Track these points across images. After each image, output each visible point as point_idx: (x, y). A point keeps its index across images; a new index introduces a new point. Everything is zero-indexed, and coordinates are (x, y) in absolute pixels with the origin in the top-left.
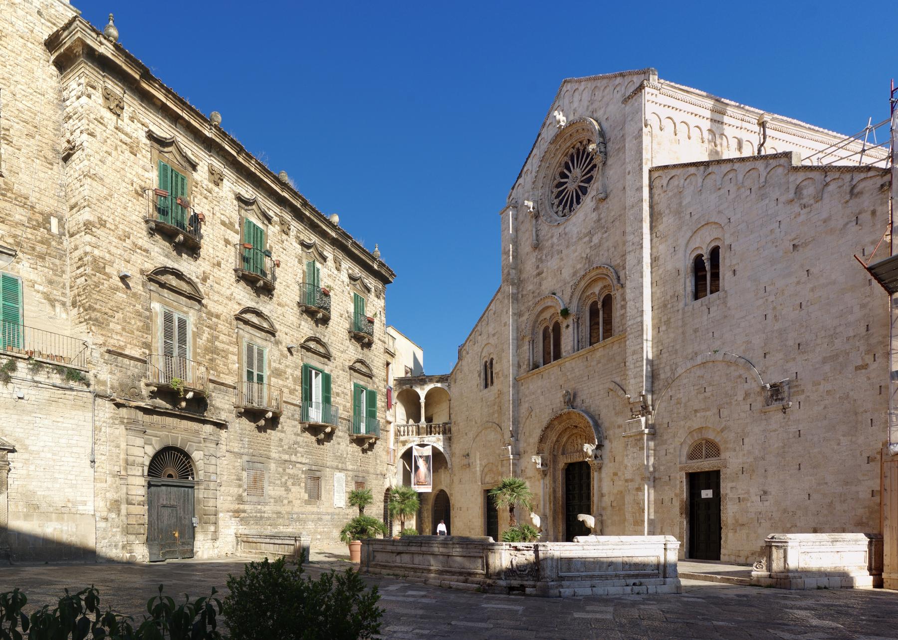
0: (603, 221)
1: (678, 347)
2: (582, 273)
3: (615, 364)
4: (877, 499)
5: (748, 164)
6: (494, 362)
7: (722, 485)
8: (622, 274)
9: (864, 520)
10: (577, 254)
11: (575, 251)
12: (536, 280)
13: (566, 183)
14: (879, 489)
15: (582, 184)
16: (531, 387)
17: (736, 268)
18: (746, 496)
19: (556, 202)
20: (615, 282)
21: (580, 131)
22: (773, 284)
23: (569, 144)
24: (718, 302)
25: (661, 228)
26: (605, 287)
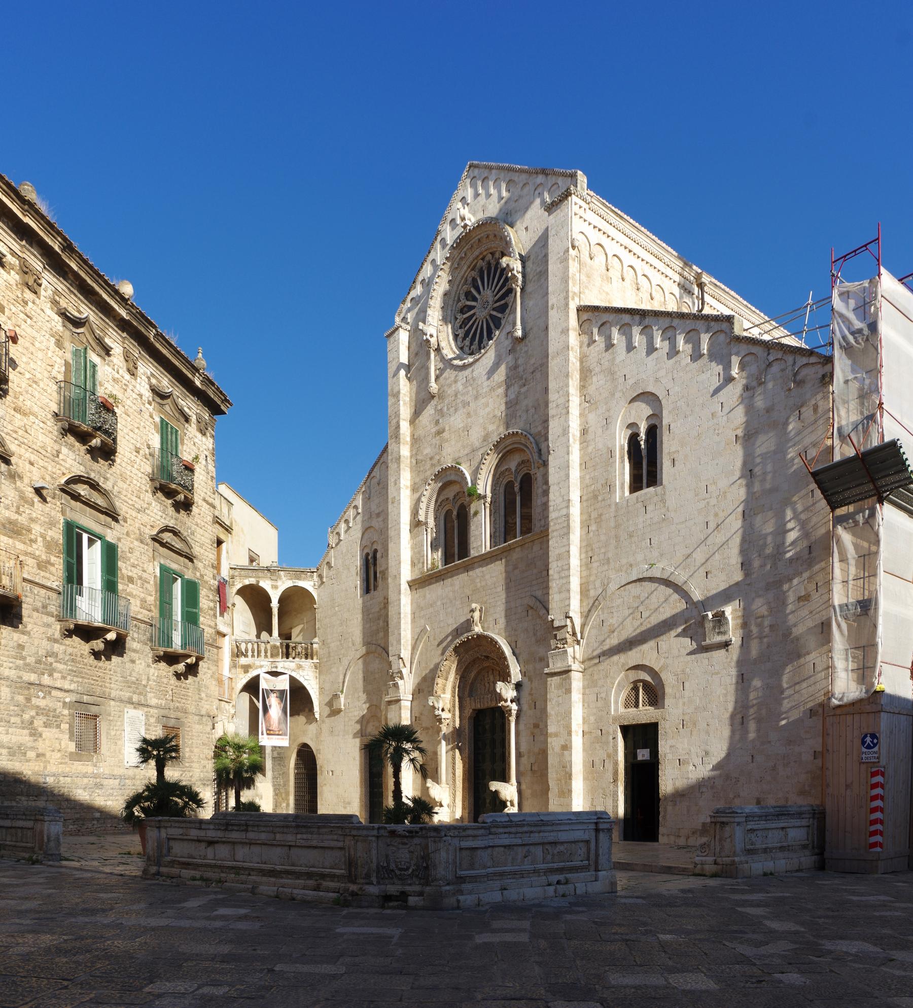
0: (521, 369)
1: (610, 555)
3: (535, 571)
4: (819, 762)
5: (688, 322)
6: (379, 555)
7: (661, 743)
8: (543, 446)
9: (807, 788)
10: (487, 410)
11: (487, 405)
12: (436, 441)
13: (473, 307)
14: (820, 749)
15: (494, 313)
16: (428, 596)
17: (675, 456)
18: (687, 757)
19: (461, 332)
20: (536, 456)
21: (491, 237)
22: (715, 483)
23: (477, 253)
24: (655, 499)
25: (591, 389)
26: (523, 462)
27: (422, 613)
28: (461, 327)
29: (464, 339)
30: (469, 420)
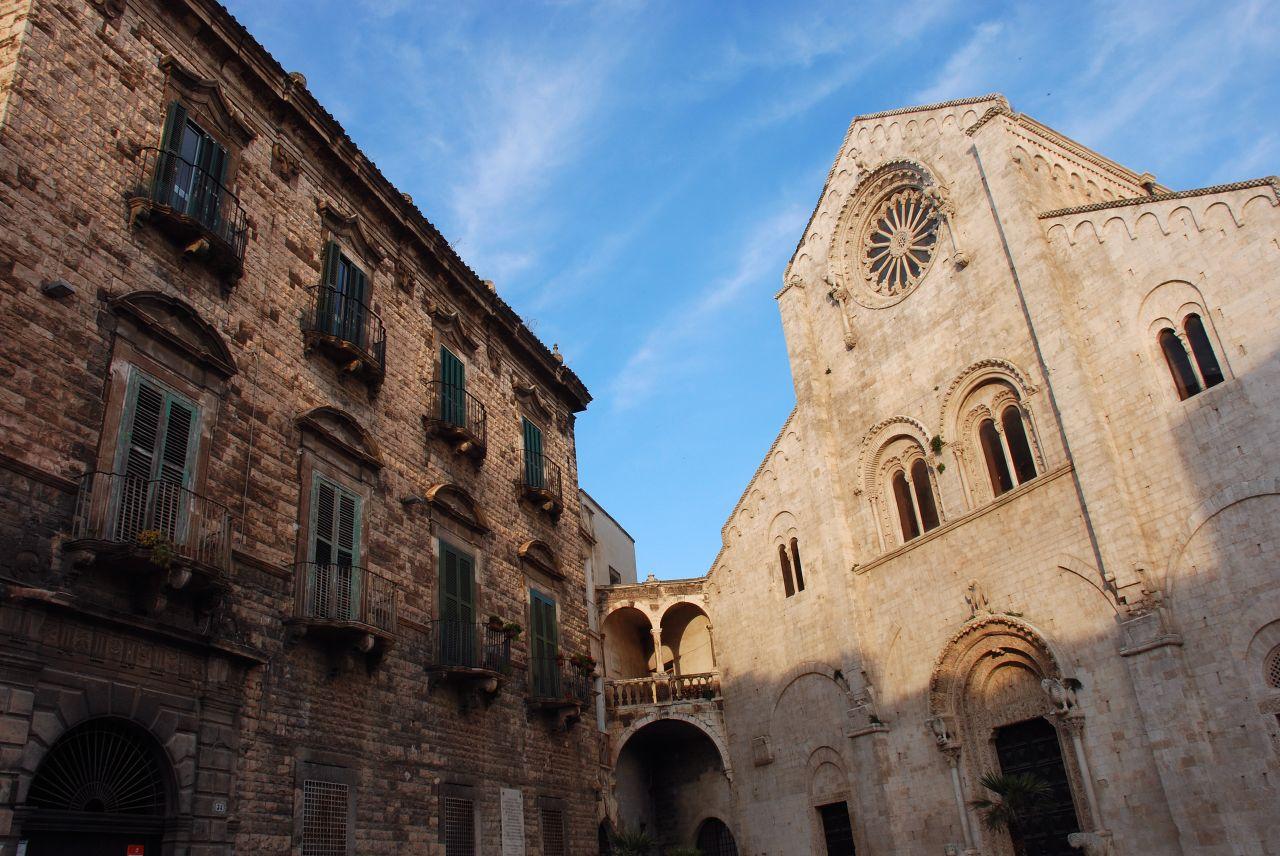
0: (973, 294)
2: (954, 376)
27: (884, 607)
28: (872, 271)
29: (879, 281)
30: (909, 364)
